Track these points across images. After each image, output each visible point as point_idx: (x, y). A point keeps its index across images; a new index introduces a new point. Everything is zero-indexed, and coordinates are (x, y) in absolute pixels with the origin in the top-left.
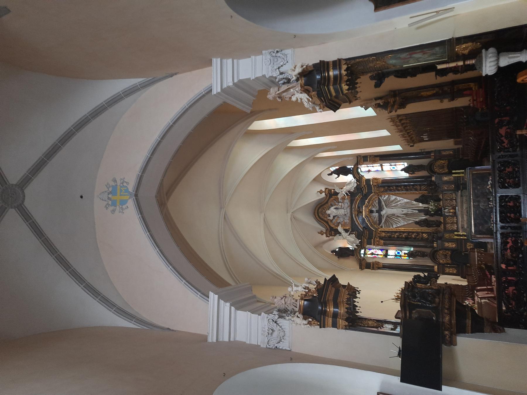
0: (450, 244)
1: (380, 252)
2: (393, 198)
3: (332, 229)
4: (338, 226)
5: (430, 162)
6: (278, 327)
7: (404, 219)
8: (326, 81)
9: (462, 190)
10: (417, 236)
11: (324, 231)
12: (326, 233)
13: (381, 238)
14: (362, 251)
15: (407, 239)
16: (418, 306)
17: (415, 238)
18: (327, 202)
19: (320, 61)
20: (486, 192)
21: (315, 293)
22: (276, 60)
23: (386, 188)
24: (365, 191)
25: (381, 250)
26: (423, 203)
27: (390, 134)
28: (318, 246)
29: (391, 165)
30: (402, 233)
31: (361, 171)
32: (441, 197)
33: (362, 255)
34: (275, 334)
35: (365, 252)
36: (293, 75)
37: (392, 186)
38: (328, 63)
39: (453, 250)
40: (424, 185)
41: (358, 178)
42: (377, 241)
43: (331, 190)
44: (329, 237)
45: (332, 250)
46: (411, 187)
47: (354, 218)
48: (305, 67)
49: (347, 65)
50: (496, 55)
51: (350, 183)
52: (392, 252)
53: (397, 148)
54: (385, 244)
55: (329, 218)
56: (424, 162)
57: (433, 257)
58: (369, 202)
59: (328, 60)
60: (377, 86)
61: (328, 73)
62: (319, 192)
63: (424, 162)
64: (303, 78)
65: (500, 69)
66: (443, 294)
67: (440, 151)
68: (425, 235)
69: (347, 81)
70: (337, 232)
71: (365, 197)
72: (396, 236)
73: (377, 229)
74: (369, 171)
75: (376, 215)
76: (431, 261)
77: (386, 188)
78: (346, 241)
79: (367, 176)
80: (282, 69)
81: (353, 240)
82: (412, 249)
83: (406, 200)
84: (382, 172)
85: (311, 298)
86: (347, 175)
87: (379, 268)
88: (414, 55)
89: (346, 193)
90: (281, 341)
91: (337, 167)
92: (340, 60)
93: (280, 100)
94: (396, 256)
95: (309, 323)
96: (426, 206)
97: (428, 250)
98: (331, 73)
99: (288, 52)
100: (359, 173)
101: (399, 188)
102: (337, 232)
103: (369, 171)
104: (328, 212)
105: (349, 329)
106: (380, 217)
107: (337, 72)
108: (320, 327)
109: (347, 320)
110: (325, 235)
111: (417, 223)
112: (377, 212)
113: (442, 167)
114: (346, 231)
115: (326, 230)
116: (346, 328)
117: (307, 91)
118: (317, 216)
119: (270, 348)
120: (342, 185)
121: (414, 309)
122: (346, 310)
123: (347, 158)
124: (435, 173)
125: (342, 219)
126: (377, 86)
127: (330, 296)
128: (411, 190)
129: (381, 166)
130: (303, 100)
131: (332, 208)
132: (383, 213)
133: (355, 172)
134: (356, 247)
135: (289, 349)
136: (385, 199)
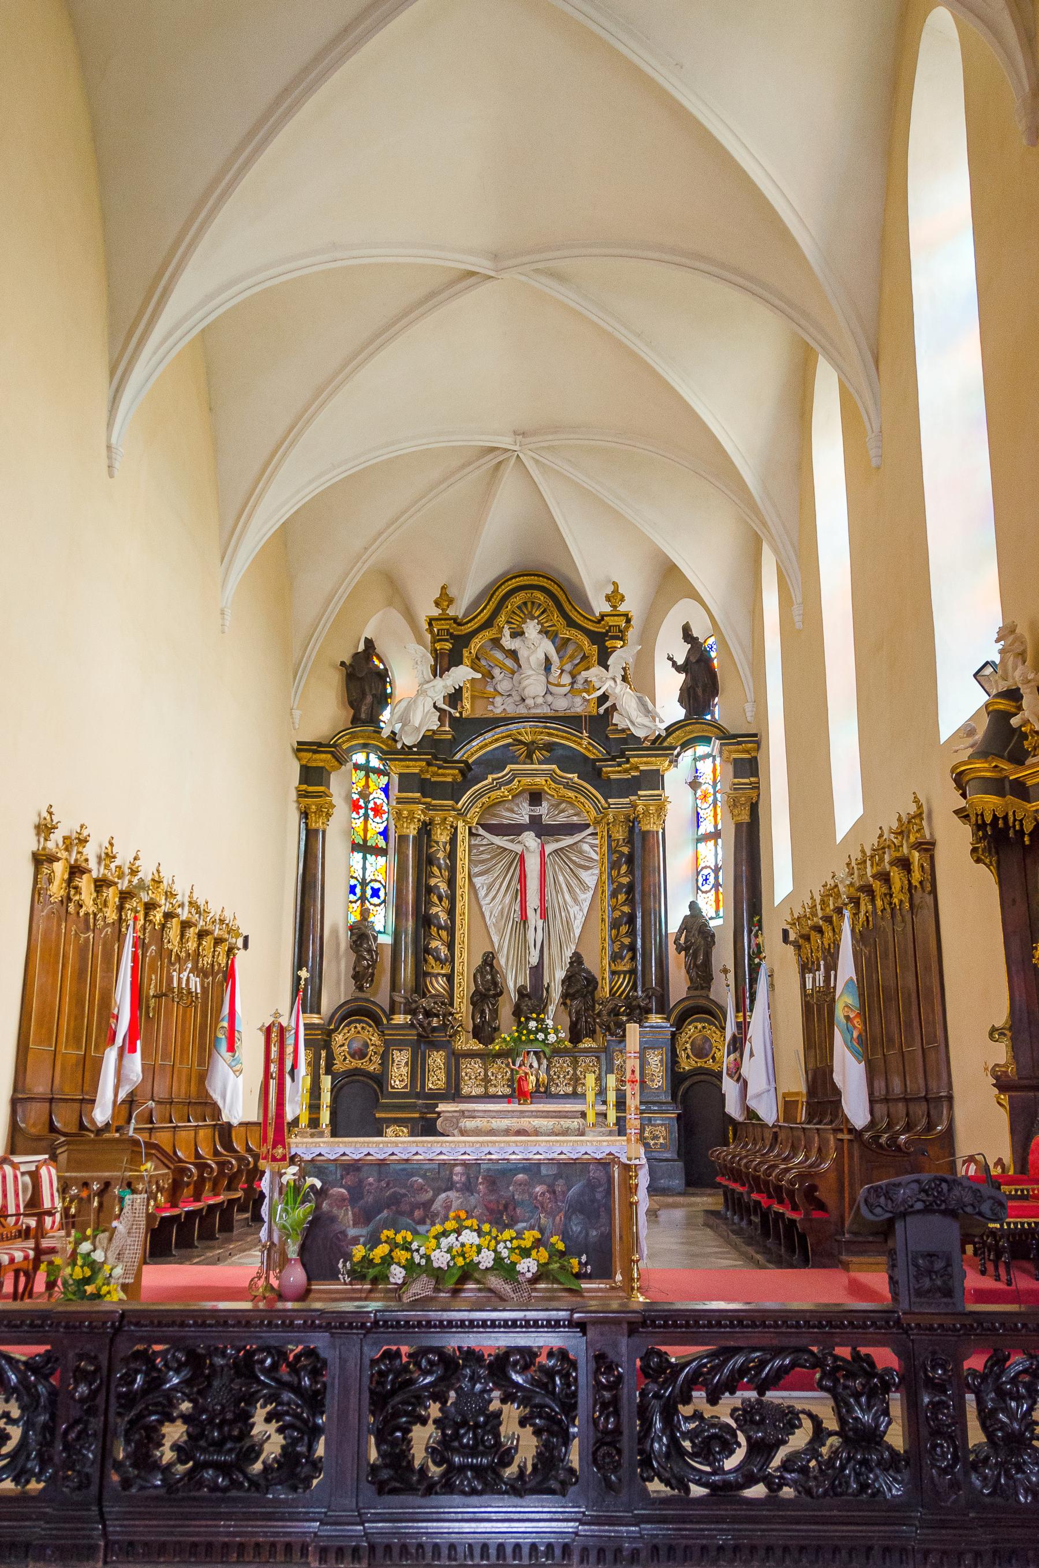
0: (404, 1070)
1: (376, 826)
2: (590, 878)
3: (461, 642)
4: (475, 667)
10: (437, 959)
11: (451, 612)
13: (426, 829)
15: (425, 921)
17: (427, 951)
18: (571, 623)
23: (626, 850)
24: (613, 772)
25: (386, 828)
26: (563, 982)
28: (393, 588)
30: (446, 903)
32: (587, 1043)
33: (360, 758)
37: (631, 871)
39: (380, 1080)
40: (634, 988)
42: (411, 813)
43: (621, 639)
44: (431, 632)
46: (627, 941)
52: (378, 869)
54: (402, 839)
55: (507, 632)
57: (355, 1012)
68: (438, 985)
70: (444, 662)
71: (592, 772)
73: (461, 814)
74: (694, 784)
75: (523, 813)
77: (626, 850)
78: (415, 697)
79: (675, 778)
81: (416, 719)
84: (690, 835)
86: (681, 701)
87: (305, 814)
89: (603, 698)
94: (364, 883)
96: (556, 992)
100: (685, 745)
101: (622, 897)
102: (444, 662)
103: (694, 784)
104: (532, 629)
106: (513, 830)
110: (436, 612)
111: (489, 961)
114: (455, 697)
115: (455, 620)
120: (641, 679)
123: (750, 696)
125: (504, 686)
129: (716, 835)
131: (547, 647)
134: (386, 733)
136: (586, 847)
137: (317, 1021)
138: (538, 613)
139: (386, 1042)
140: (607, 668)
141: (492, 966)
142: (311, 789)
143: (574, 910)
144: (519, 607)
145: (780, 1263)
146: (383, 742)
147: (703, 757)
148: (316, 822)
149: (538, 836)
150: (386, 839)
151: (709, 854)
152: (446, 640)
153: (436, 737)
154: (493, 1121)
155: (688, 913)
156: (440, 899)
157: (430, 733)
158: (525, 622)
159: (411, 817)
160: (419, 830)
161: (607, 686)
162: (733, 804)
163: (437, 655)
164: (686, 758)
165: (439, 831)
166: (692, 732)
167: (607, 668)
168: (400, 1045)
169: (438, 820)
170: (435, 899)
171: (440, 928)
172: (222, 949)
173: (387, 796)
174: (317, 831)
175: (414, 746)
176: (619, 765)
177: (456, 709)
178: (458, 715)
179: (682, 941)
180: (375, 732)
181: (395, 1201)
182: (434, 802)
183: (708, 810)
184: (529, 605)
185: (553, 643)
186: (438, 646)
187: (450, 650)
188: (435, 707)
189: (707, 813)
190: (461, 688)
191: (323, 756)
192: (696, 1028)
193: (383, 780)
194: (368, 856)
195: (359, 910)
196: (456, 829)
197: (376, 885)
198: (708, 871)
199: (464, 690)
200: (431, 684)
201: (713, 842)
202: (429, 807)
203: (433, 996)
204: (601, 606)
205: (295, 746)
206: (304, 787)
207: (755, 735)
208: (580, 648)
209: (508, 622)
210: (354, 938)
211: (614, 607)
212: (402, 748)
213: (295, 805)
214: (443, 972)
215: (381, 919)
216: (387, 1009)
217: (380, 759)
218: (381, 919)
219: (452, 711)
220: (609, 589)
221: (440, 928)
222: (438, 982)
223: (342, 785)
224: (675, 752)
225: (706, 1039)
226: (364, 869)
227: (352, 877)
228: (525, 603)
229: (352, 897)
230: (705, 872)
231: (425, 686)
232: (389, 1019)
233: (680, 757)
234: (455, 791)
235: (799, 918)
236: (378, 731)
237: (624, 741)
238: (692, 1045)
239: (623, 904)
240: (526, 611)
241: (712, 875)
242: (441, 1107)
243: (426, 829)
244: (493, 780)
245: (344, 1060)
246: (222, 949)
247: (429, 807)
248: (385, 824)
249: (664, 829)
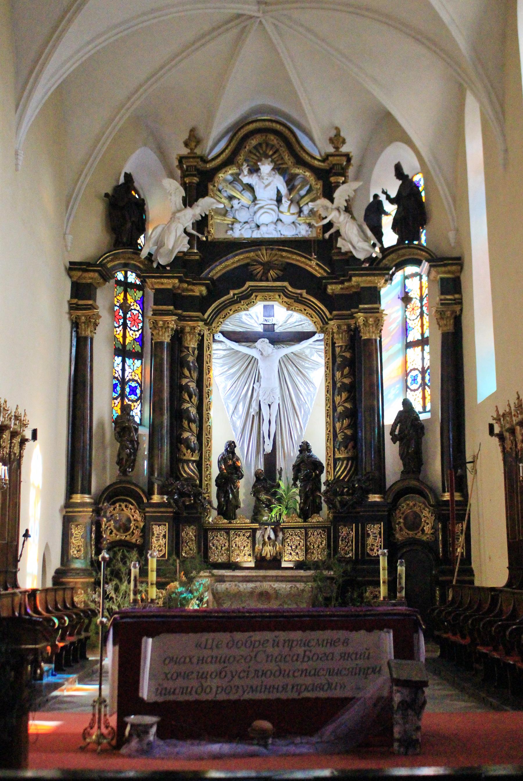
10: (188, 447)
12: (192, 156)
13: (178, 337)
18: (300, 162)
25: (142, 335)
29: (423, 372)
30: (195, 400)
31: (406, 278)
33: (120, 276)
35: (133, 286)
41: (383, 265)
45: (135, 177)
53: (485, 382)
54: (157, 346)
62: (338, 135)
68: (190, 470)
72: (184, 381)
74: (406, 299)
76: (108, 484)
79: (389, 294)
81: (170, 243)
87: (75, 325)
89: (330, 225)
91: (424, 200)
94: (123, 382)
100: (400, 266)
102: (193, 195)
103: (406, 299)
110: (185, 151)
114: (202, 224)
129: (423, 342)
132: (263, 344)
134: (144, 254)
137: (88, 500)
138: (271, 153)
139: (145, 518)
140: (332, 200)
141: (233, 453)
142: (81, 302)
144: (255, 147)
145: (515, 710)
146: (140, 262)
148: (85, 331)
150: (142, 345)
151: (417, 358)
152: (194, 175)
153: (187, 257)
154: (240, 584)
155: (401, 408)
156: (190, 397)
157: (181, 254)
158: (260, 160)
159: (166, 326)
160: (173, 338)
161: (333, 216)
162: (440, 315)
164: (398, 276)
165: (189, 338)
166: (404, 255)
167: (332, 200)
168: (159, 520)
169: (188, 329)
170: (186, 397)
171: (190, 420)
172: (17, 441)
173: (143, 309)
174: (86, 338)
175: (168, 265)
176: (342, 283)
177: (203, 234)
178: (204, 239)
179: (397, 433)
180: (134, 253)
182: (185, 313)
183: (416, 321)
184: (264, 146)
185: (284, 178)
186: (187, 180)
187: (198, 184)
188: (185, 231)
189: (415, 325)
190: (206, 216)
191: (91, 274)
192: (408, 505)
193: (139, 294)
194: (127, 359)
195: (119, 406)
196: (203, 336)
197: (134, 384)
198: (417, 372)
199: (210, 218)
200: (183, 213)
201: (420, 348)
202: (181, 318)
203: (186, 479)
205: (68, 265)
206: (75, 301)
207: (459, 259)
209: (246, 160)
210: (118, 429)
211: (337, 148)
212: (157, 267)
213: (67, 316)
214: (193, 459)
216: (146, 489)
217: (138, 276)
219: (200, 236)
220: (333, 133)
221: (190, 420)
222: (189, 468)
223: (107, 298)
224: (391, 272)
226: (123, 370)
227: (115, 378)
228: (260, 144)
229: (115, 395)
230: (414, 373)
231: (178, 215)
232: (149, 498)
233: (394, 277)
234: (202, 304)
235: (504, 415)
236: (137, 251)
237: (347, 261)
238: (405, 519)
239: (345, 401)
241: (420, 376)
243: (178, 337)
244: (234, 295)
245: (111, 533)
246: (17, 441)
247: (181, 318)
248: (140, 331)
249: (381, 337)
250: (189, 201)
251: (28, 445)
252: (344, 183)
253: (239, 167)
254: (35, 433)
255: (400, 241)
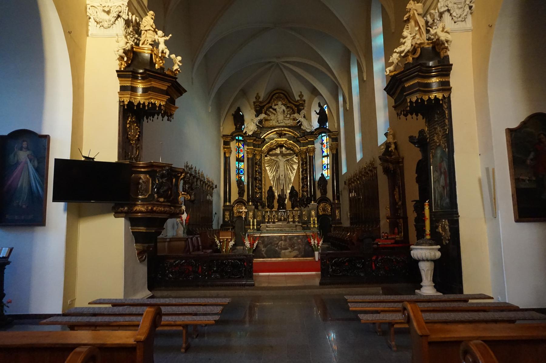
2: (295, 167)
4: (266, 113)
5: (329, 200)
6: (113, 20)
7: (274, 177)
8: (426, 73)
9: (301, 226)
13: (254, 155)
14: (241, 138)
16: (154, 180)
17: (256, 186)
18: (290, 102)
19: (452, 65)
20: (294, 247)
21: (159, 65)
22: (460, 6)
27: (358, 161)
31: (322, 136)
33: (237, 138)
34: (105, 16)
35: (241, 140)
36: (437, 31)
38: (448, 75)
40: (308, 195)
47: (273, 130)
48: (446, 45)
49: (442, 100)
50: (433, 258)
51: (311, 126)
56: (330, 195)
57: (240, 202)
58: (290, 144)
59: (451, 75)
60: (412, 139)
61: (434, 76)
63: (330, 195)
64: (431, 45)
65: (416, 262)
66: (169, 206)
67: (339, 208)
69: (422, 99)
70: (258, 114)
71: (297, 141)
80: (446, 16)
82: (245, 183)
83: (292, 179)
85: (154, 61)
86: (318, 122)
88: (443, 176)
89: (299, 122)
90: (97, 23)
92: (450, 90)
93: (405, 19)
95: (121, 58)
96: (288, 196)
97: (245, 198)
98: (434, 80)
99: (469, 24)
100: (319, 134)
101: (304, 172)
102: (258, 114)
103: (322, 144)
105: (120, 106)
107: (434, 87)
108: (117, 71)
109: (130, 103)
111: (271, 188)
112: (281, 152)
113: (324, 210)
114: (261, 122)
116: (121, 102)
117: (414, 50)
118: (275, 92)
119: (86, 8)
120: (308, 118)
121: (150, 176)
122: (142, 102)
124: (319, 203)
126: (412, 139)
127: (155, 84)
128: (302, 183)
129: (327, 156)
130: (402, 46)
131: (284, 108)
132: (280, 157)
133: (322, 129)
134: (244, 132)
135: (90, 33)
136: (294, 159)
143: (291, 175)
147: (324, 136)
149: (282, 156)
151: (326, 161)
161: (300, 119)
163: (256, 111)
181: (271, 243)
189: (325, 150)
204: (297, 98)
208: (291, 108)
215: (244, 178)
218: (244, 178)
220: (300, 94)
223: (233, 145)
225: (326, 207)
240: (279, 98)
242: (261, 225)
243: (254, 155)
250: (257, 116)
251: (215, 189)
252: (303, 109)
253: (272, 104)
254: (216, 186)
255: (320, 126)
